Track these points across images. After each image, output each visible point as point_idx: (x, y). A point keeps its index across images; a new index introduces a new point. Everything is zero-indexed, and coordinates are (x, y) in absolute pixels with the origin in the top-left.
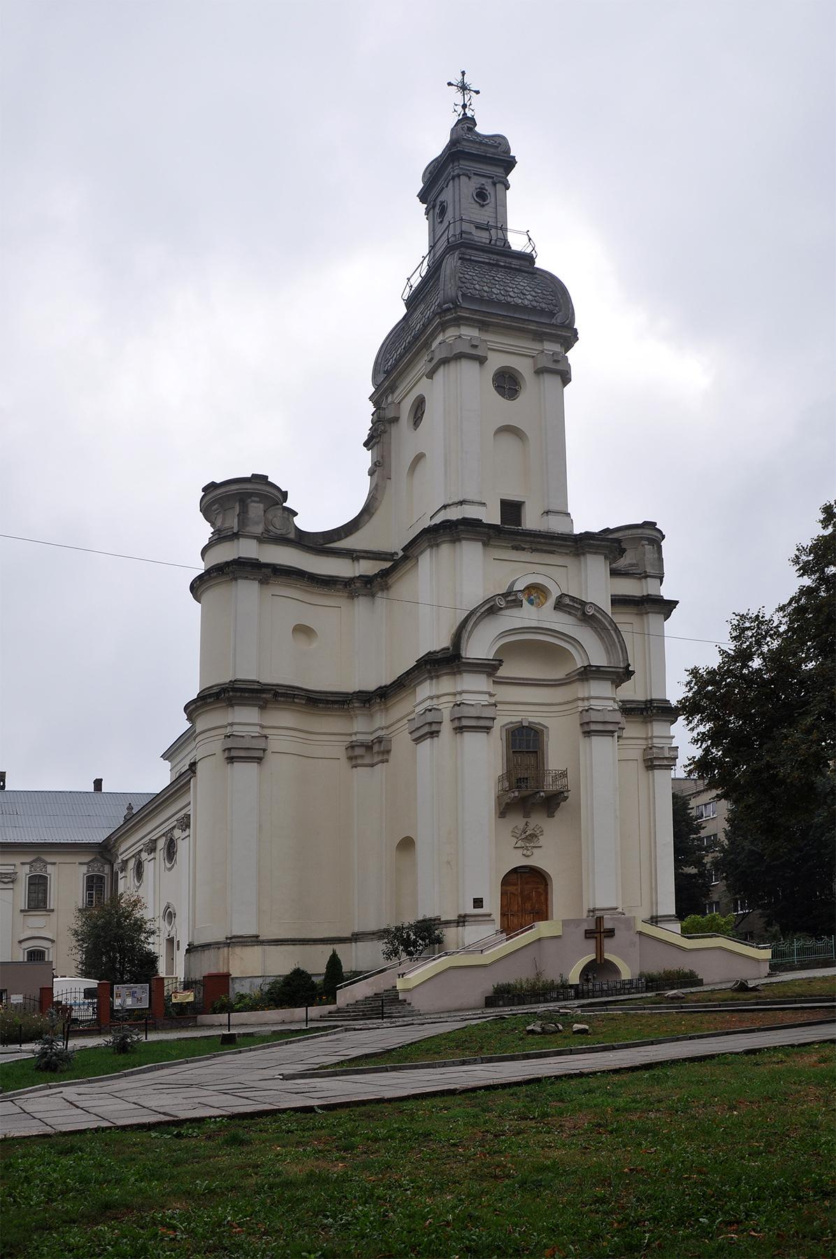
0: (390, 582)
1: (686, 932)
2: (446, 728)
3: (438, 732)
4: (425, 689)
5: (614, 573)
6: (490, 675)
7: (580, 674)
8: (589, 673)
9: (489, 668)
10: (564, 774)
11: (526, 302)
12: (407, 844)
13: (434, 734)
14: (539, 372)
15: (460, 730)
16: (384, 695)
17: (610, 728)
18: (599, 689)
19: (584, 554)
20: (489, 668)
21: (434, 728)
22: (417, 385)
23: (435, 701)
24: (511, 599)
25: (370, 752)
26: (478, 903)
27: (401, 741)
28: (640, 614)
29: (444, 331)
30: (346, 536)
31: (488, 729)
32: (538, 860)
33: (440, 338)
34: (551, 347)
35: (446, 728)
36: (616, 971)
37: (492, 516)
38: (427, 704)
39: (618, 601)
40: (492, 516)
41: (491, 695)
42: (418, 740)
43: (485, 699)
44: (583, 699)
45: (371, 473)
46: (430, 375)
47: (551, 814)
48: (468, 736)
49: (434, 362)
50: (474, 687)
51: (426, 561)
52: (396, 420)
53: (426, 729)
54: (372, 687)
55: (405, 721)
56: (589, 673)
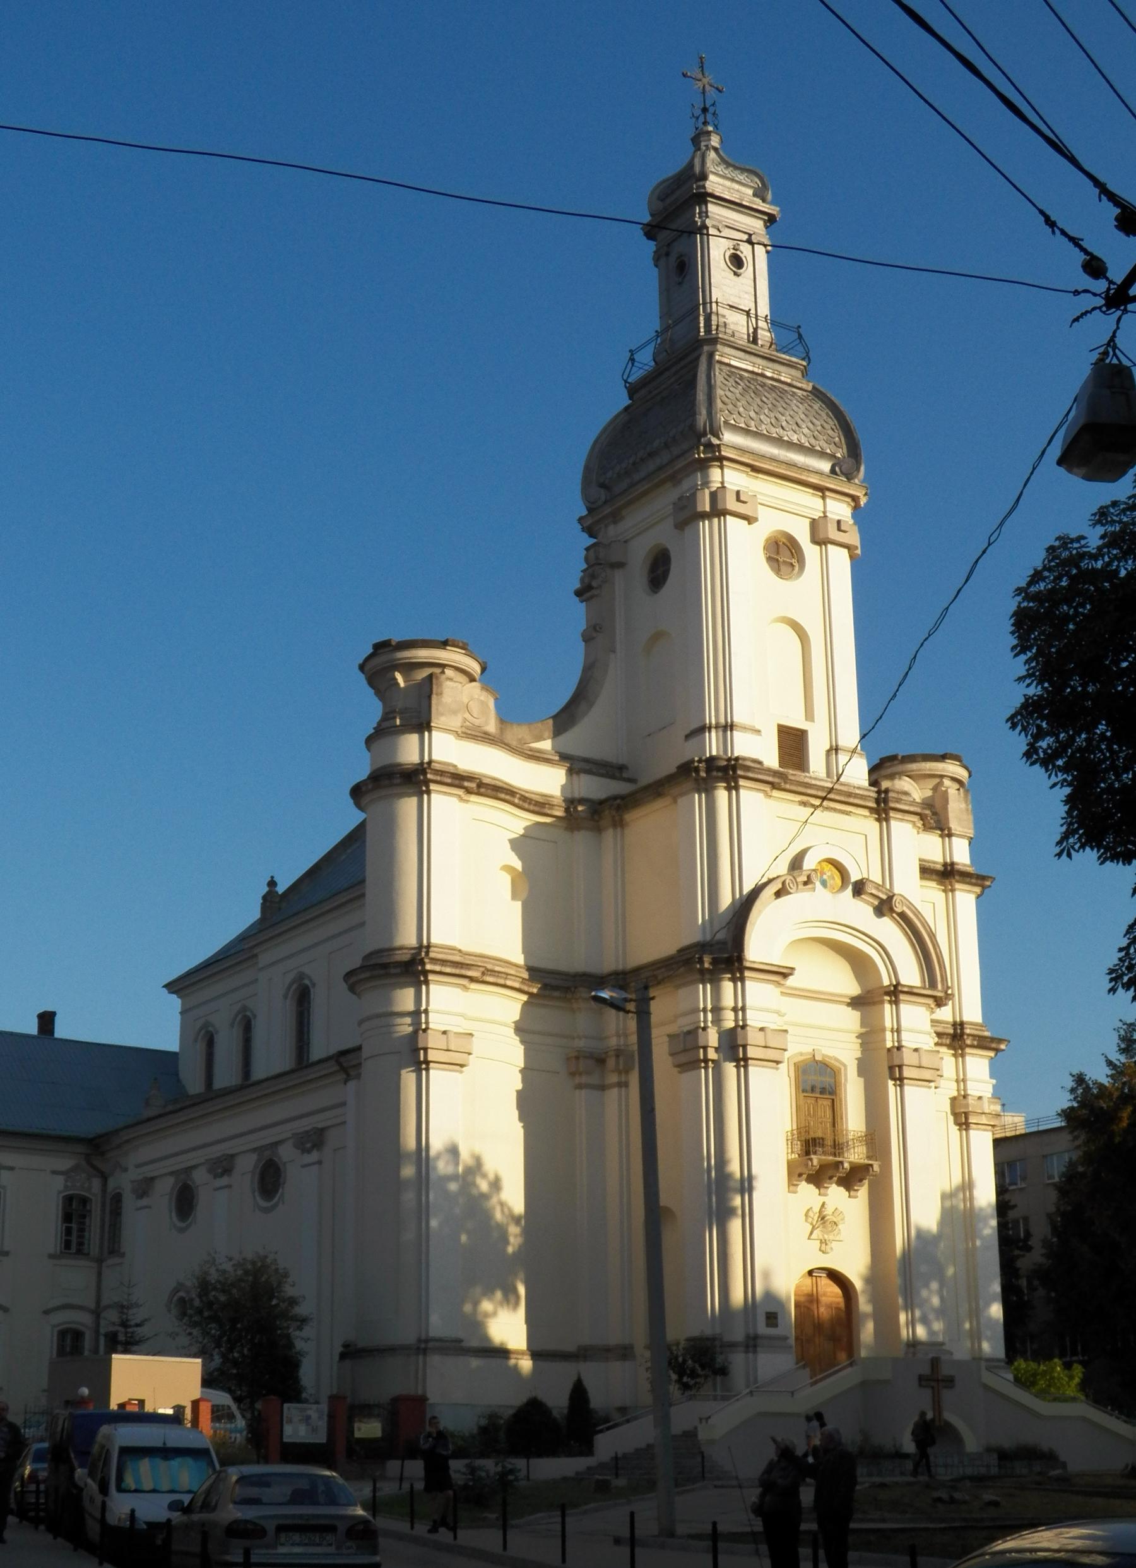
17: (927, 1074)
36: (957, 1439)
56: (895, 992)
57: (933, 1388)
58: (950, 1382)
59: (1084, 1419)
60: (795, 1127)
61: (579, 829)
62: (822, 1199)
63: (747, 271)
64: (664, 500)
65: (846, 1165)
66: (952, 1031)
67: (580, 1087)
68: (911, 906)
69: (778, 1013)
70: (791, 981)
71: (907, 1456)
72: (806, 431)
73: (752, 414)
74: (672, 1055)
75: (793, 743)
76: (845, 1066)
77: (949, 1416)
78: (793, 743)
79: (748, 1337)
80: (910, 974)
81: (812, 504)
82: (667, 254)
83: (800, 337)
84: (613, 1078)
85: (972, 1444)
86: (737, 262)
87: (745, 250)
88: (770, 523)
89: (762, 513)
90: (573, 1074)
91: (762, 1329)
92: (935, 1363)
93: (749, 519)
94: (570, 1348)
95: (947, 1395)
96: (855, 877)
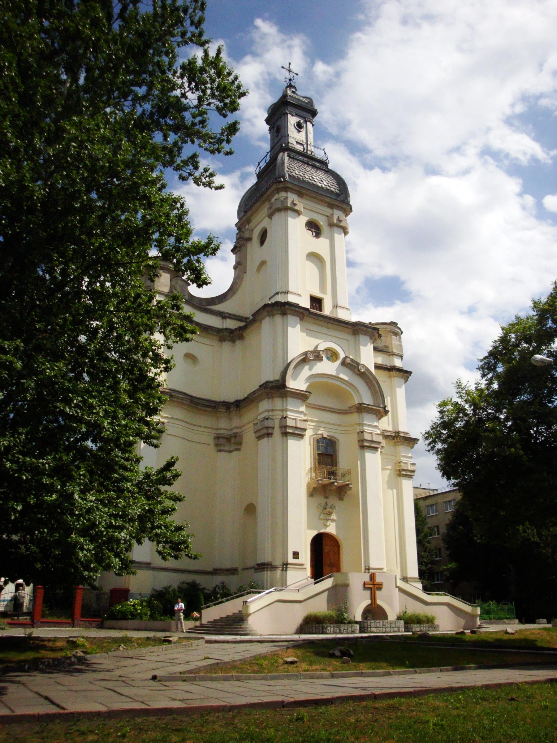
0: (244, 334)
1: (425, 589)
2: (277, 432)
4: (264, 405)
5: (376, 349)
7: (357, 408)
8: (361, 409)
9: (302, 396)
10: (349, 472)
11: (324, 186)
12: (251, 509)
13: (269, 435)
14: (331, 225)
15: (285, 434)
16: (237, 406)
18: (368, 420)
19: (358, 334)
22: (261, 221)
23: (271, 414)
24: (317, 356)
25: (228, 442)
26: (296, 555)
27: (249, 437)
28: (390, 377)
29: (278, 193)
30: (219, 303)
31: (301, 436)
32: (331, 529)
33: (276, 196)
34: (337, 214)
35: (277, 432)
37: (305, 303)
38: (266, 415)
39: (377, 367)
40: (305, 303)
42: (259, 438)
45: (235, 268)
46: (270, 216)
47: (341, 499)
49: (272, 209)
51: (266, 324)
52: (250, 239)
53: (265, 431)
54: (232, 399)
55: (251, 425)
56: (361, 409)
58: (379, 587)
59: (449, 605)
60: (313, 466)
62: (326, 500)
63: (304, 130)
64: (264, 211)
65: (336, 484)
66: (394, 435)
67: (219, 451)
68: (367, 369)
70: (309, 401)
71: (356, 622)
72: (325, 183)
73: (301, 174)
74: (255, 432)
75: (316, 302)
76: (338, 440)
77: (379, 602)
78: (316, 302)
79: (284, 564)
80: (367, 400)
81: (328, 211)
82: (273, 128)
83: (325, 153)
84: (233, 447)
85: (392, 617)
90: (217, 445)
91: (291, 560)
92: (372, 577)
94: (210, 569)
95: (378, 593)
96: (342, 355)
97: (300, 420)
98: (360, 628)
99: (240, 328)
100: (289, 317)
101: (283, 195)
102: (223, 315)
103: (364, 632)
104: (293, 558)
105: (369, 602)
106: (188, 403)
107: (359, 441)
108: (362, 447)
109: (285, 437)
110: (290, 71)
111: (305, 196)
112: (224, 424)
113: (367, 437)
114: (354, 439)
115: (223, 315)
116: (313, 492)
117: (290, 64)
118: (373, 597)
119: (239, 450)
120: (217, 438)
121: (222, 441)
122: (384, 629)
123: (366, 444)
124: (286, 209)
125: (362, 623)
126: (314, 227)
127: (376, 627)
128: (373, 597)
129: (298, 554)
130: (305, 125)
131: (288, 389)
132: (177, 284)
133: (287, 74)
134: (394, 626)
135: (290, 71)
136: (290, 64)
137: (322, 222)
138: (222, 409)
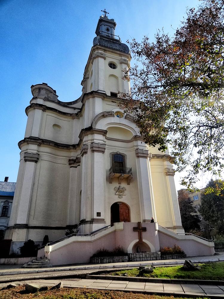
2: (89, 151)
3: (87, 152)
6: (104, 135)
11: (117, 48)
13: (86, 153)
15: (93, 151)
20: (104, 133)
21: (86, 151)
26: (99, 214)
31: (103, 152)
35: (89, 151)
41: (104, 142)
43: (102, 142)
44: (136, 146)
48: (96, 153)
50: (98, 138)
57: (138, 231)
58: (145, 229)
61: (75, 118)
67: (71, 167)
69: (103, 141)
70: (107, 135)
76: (126, 155)
86: (108, 30)
87: (110, 28)
88: (109, 60)
89: (107, 58)
90: (70, 164)
91: (95, 217)
93: (105, 59)
94: (64, 226)
95: (144, 234)
97: (101, 144)
98: (129, 258)
99: (80, 112)
100: (96, 98)
101: (96, 51)
102: (75, 108)
103: (132, 261)
104: (97, 216)
105: (138, 240)
106: (53, 145)
107: (136, 154)
108: (138, 157)
109: (93, 153)
110: (105, 12)
111: (107, 52)
112: (73, 154)
113: (139, 151)
114: (133, 153)
115: (75, 108)
116: (110, 179)
117: (105, 9)
118: (140, 238)
119: (80, 165)
120: (70, 160)
121: (72, 162)
122: (146, 258)
123: (140, 155)
124: (98, 56)
125: (130, 255)
126: (112, 66)
127: (140, 258)
128: (140, 238)
129: (100, 214)
130: (111, 29)
131: (93, 129)
132: (51, 96)
133: (104, 14)
134: (152, 256)
135: (105, 12)
136: (105, 9)
137: (116, 62)
138: (71, 147)
